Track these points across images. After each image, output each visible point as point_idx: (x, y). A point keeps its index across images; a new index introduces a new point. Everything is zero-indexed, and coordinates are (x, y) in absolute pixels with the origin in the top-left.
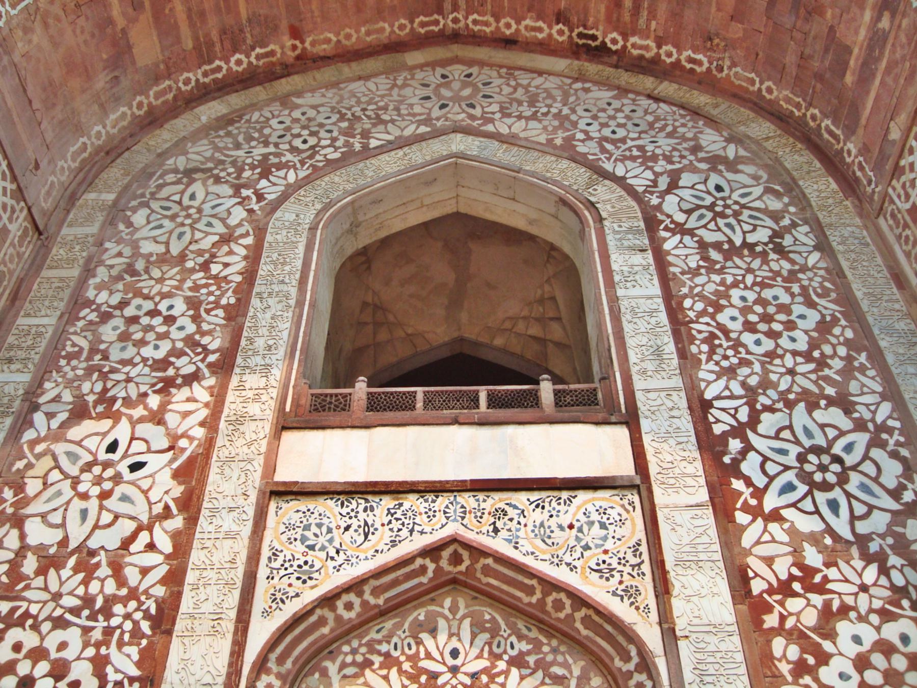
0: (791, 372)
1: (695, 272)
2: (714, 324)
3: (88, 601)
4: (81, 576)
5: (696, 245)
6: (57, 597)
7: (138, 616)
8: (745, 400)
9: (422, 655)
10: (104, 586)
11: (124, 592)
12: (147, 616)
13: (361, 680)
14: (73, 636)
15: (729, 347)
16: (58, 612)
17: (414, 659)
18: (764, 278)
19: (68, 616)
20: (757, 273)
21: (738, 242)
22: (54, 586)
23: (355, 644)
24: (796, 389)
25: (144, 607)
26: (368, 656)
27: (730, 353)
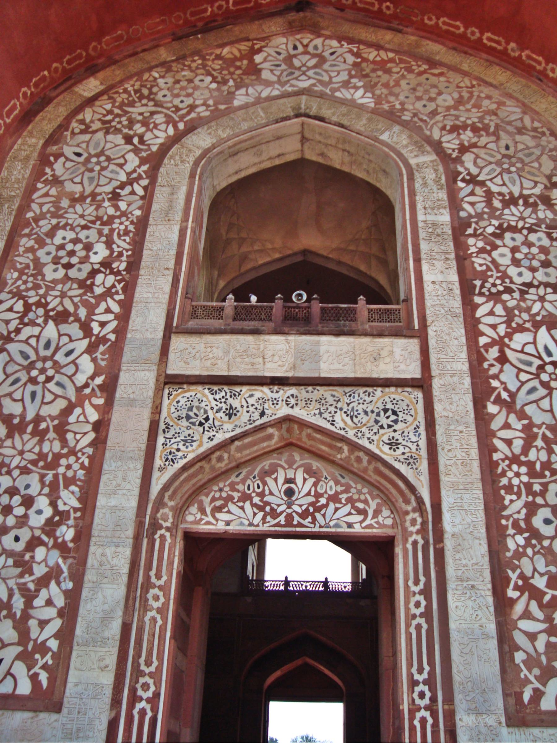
0: (542, 299)
1: (480, 216)
2: (490, 259)
3: (42, 456)
4: (36, 439)
5: (484, 195)
6: (21, 453)
7: (76, 466)
8: (505, 319)
9: (267, 492)
10: (52, 446)
11: (65, 451)
12: (82, 467)
13: (226, 509)
14: (34, 480)
15: (498, 278)
16: (23, 463)
17: (262, 495)
18: (532, 224)
19: (29, 466)
20: (527, 220)
21: (516, 195)
22: (19, 446)
23: (221, 485)
24: (543, 313)
25: (80, 461)
26: (230, 493)
27: (498, 282)
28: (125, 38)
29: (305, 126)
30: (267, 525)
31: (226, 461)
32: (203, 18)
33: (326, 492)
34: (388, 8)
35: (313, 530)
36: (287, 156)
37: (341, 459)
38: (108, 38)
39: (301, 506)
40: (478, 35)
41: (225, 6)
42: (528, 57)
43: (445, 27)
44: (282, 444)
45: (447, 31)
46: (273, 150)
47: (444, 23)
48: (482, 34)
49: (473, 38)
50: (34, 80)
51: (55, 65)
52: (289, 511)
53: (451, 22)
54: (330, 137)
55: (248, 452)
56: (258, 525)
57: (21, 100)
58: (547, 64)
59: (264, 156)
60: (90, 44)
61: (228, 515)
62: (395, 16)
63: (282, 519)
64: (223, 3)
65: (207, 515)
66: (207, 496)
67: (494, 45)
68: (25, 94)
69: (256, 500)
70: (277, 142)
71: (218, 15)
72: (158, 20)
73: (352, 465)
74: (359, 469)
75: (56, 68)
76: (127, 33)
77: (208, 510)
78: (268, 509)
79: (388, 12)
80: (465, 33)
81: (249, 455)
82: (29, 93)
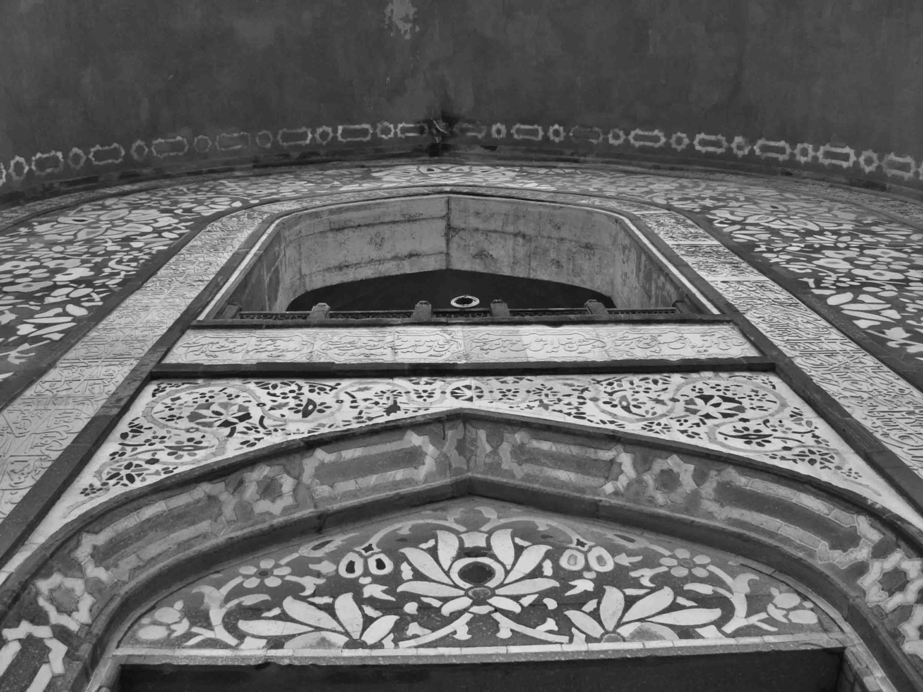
23: (266, 564)
28: (186, 148)
29: (453, 206)
30: (413, 642)
31: (288, 500)
32: (300, 146)
33: (587, 568)
34: (557, 133)
35: (567, 648)
36: (424, 260)
37: (616, 493)
38: (160, 140)
39: (516, 598)
40: (686, 141)
41: (331, 135)
42: (764, 149)
43: (638, 144)
44: (447, 480)
45: (643, 149)
46: (402, 241)
47: (637, 138)
48: (692, 139)
49: (679, 148)
50: (39, 155)
51: (75, 150)
52: (482, 610)
53: (646, 133)
54: (492, 215)
55: (349, 485)
56: (379, 645)
57: (11, 170)
58: (793, 146)
59: (386, 252)
60: (133, 141)
61: (280, 624)
62: (567, 143)
63: (461, 629)
64: (329, 130)
65: (209, 626)
66: (218, 585)
67: (711, 149)
68: (18, 166)
69: (375, 591)
70: (408, 226)
71: (321, 146)
72: (235, 135)
73: (652, 501)
74: (673, 507)
75: (77, 157)
76: (191, 144)
77: (216, 616)
78: (411, 608)
79: (557, 140)
80: (667, 144)
81: (354, 494)
82: (26, 169)
